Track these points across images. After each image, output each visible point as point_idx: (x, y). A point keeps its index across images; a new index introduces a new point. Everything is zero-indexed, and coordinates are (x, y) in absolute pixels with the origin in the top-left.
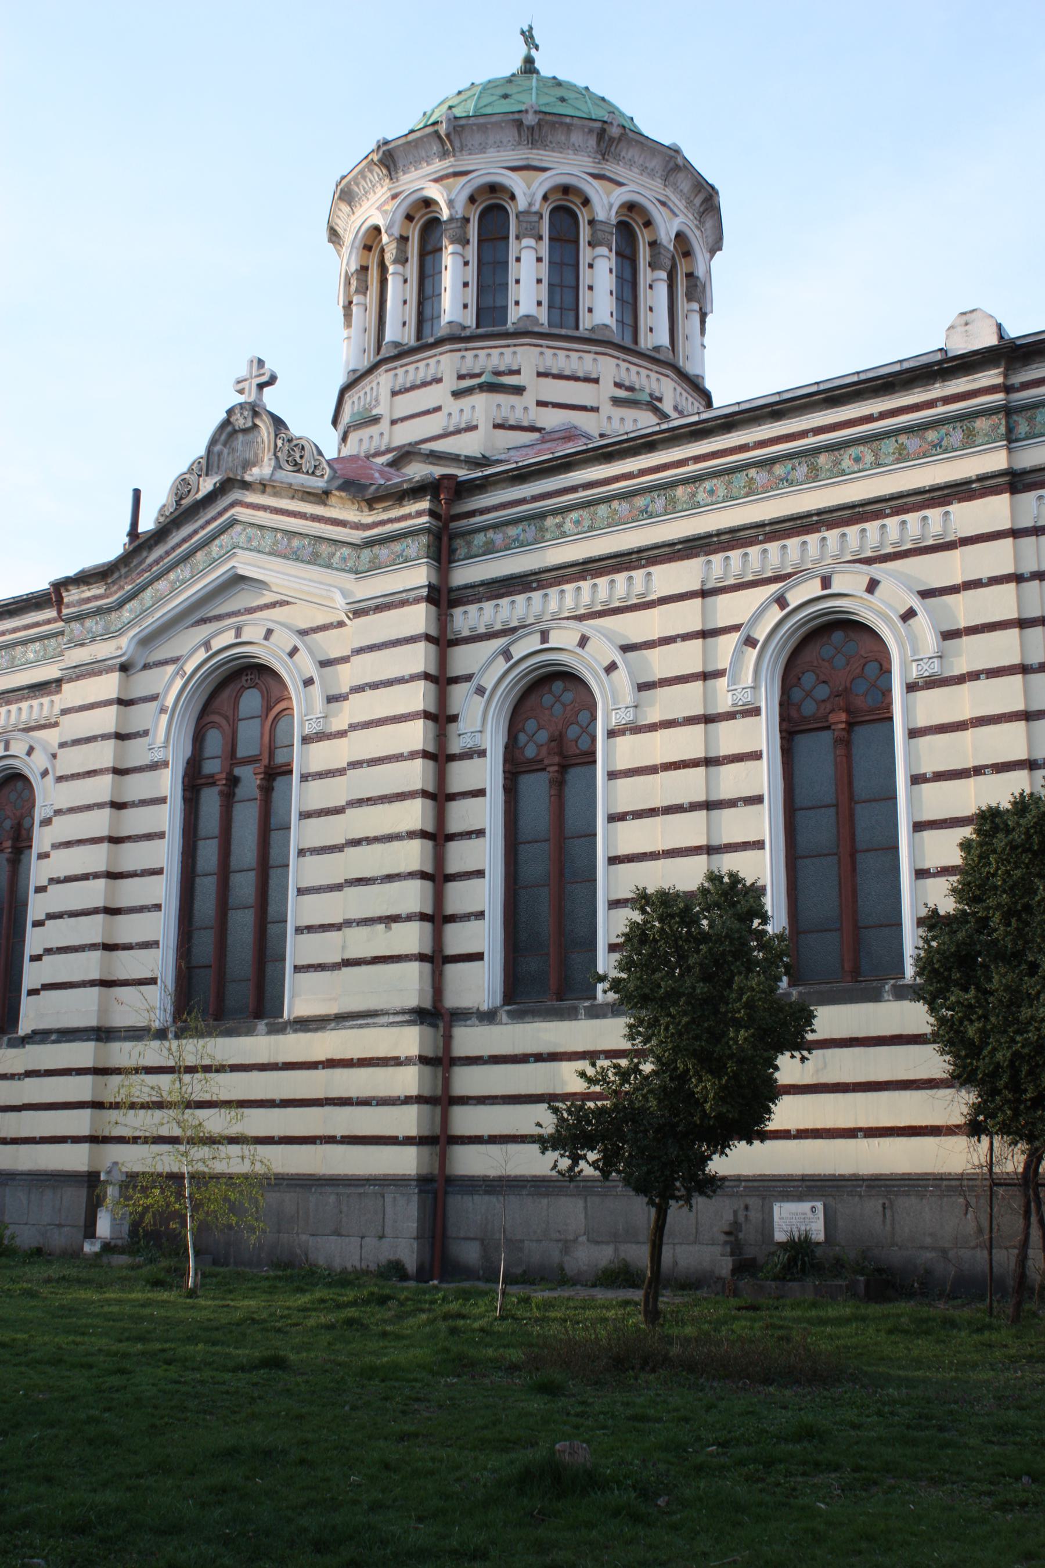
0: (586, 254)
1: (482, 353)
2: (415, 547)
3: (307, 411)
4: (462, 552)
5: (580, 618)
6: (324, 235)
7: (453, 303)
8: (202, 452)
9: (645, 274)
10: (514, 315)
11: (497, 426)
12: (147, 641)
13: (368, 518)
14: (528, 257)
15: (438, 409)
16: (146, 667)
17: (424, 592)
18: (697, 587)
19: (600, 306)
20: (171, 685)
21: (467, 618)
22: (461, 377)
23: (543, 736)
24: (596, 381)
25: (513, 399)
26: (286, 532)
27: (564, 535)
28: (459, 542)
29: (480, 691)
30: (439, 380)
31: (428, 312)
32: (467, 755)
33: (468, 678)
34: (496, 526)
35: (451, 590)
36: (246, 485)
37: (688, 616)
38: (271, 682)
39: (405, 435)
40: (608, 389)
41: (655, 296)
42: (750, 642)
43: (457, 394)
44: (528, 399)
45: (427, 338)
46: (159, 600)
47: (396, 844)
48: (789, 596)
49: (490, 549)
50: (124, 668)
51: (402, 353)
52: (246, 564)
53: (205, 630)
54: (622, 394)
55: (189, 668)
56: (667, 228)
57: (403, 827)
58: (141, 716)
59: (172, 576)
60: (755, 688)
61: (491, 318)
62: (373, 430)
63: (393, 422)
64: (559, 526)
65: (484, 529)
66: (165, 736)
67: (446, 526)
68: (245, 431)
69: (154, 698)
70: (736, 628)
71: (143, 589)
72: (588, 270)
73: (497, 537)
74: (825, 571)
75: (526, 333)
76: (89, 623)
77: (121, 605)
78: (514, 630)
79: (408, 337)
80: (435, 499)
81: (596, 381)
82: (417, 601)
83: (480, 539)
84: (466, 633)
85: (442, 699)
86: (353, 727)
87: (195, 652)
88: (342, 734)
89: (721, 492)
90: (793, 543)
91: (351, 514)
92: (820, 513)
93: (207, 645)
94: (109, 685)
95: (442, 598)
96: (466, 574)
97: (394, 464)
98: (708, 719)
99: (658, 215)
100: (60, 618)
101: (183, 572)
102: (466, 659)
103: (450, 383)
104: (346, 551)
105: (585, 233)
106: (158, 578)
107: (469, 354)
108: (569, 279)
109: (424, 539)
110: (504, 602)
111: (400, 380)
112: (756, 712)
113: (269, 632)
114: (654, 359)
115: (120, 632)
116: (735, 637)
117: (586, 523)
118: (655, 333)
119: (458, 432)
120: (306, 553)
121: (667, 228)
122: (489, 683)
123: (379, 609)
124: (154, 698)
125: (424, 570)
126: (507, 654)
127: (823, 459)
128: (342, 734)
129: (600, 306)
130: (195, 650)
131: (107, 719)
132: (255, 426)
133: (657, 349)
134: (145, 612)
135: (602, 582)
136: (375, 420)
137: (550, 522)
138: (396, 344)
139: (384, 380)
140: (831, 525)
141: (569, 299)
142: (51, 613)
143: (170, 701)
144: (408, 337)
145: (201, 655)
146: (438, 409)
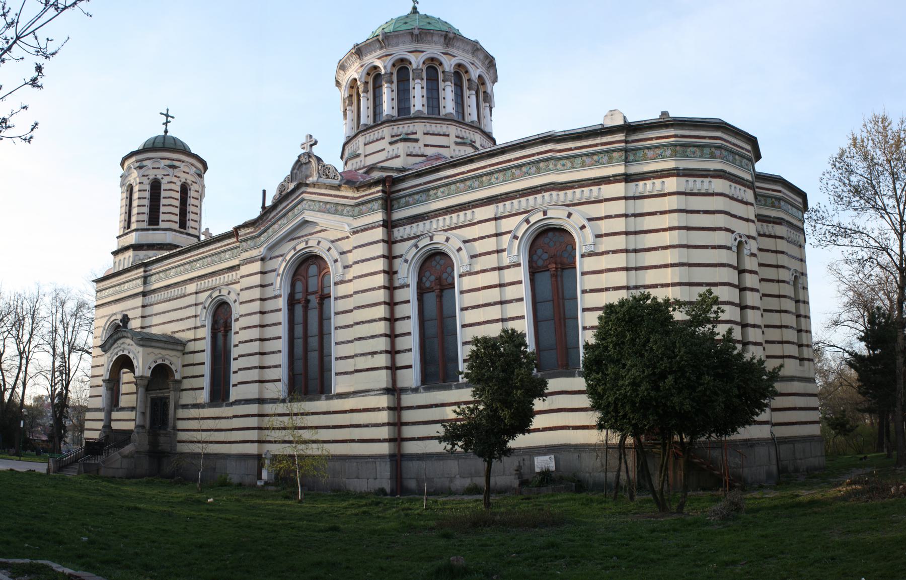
0: (441, 85)
1: (401, 126)
2: (376, 205)
3: (330, 154)
4: (396, 206)
5: (446, 230)
6: (334, 83)
7: (388, 106)
8: (289, 173)
9: (466, 92)
10: (413, 111)
11: (408, 155)
12: (271, 248)
13: (357, 195)
14: (418, 87)
15: (384, 150)
16: (271, 258)
17: (381, 223)
18: (493, 216)
19: (448, 105)
20: (281, 265)
21: (399, 233)
22: (392, 136)
23: (433, 278)
24: (448, 135)
25: (414, 144)
26: (324, 202)
27: (438, 197)
28: (395, 202)
29: (406, 261)
30: (383, 138)
31: (378, 111)
32: (402, 287)
33: (401, 256)
34: (409, 195)
35: (392, 221)
36: (307, 185)
37: (490, 228)
38: (321, 262)
39: (370, 161)
40: (452, 139)
41: (471, 101)
42: (516, 237)
43: (391, 143)
44: (421, 144)
45: (378, 121)
46: (275, 232)
47: (374, 323)
48: (530, 219)
49: (407, 204)
50: (262, 259)
51: (368, 128)
52: (308, 216)
53: (293, 243)
54: (459, 140)
55: (288, 258)
56: (474, 73)
57: (377, 316)
58: (270, 278)
59: (279, 223)
60: (518, 255)
61: (404, 112)
62: (358, 160)
63: (366, 156)
64: (436, 194)
65: (405, 196)
66: (280, 285)
67: (389, 196)
68: (306, 164)
69: (274, 270)
70: (510, 232)
71: (268, 228)
73: (410, 200)
74: (545, 209)
75: (418, 117)
76: (249, 242)
77: (260, 235)
78: (419, 236)
79: (370, 122)
80: (384, 185)
81: (448, 135)
82: (378, 226)
83: (403, 201)
84: (399, 238)
85: (391, 265)
86: (355, 278)
87: (289, 252)
88: (350, 281)
89: (501, 179)
90: (531, 198)
91: (350, 193)
92: (541, 186)
93: (294, 248)
94: (257, 266)
95: (389, 225)
96: (397, 215)
97: (367, 173)
98: (500, 269)
99: (471, 68)
100: (238, 241)
101: (284, 221)
102: (399, 249)
103: (388, 139)
104: (348, 208)
105: (441, 76)
106: (274, 224)
107: (395, 127)
108: (435, 95)
109: (380, 202)
110: (414, 225)
111: (368, 139)
112: (519, 265)
113: (319, 242)
114: (472, 126)
115: (260, 246)
116: (509, 236)
117: (447, 193)
118: (471, 115)
119: (392, 158)
120: (332, 210)
121: (474, 73)
122: (409, 257)
123: (363, 230)
124: (274, 270)
125: (381, 214)
126: (416, 246)
127: (541, 165)
128: (350, 281)
130: (290, 251)
131: (257, 280)
132: (310, 161)
133: (472, 122)
134: (269, 237)
135: (454, 216)
136: (358, 156)
137: (432, 192)
138: (365, 125)
139: (361, 140)
140: (546, 191)
141: (435, 103)
142: (234, 240)
143: (281, 271)
144: (370, 122)
145: (293, 253)
146: (384, 150)
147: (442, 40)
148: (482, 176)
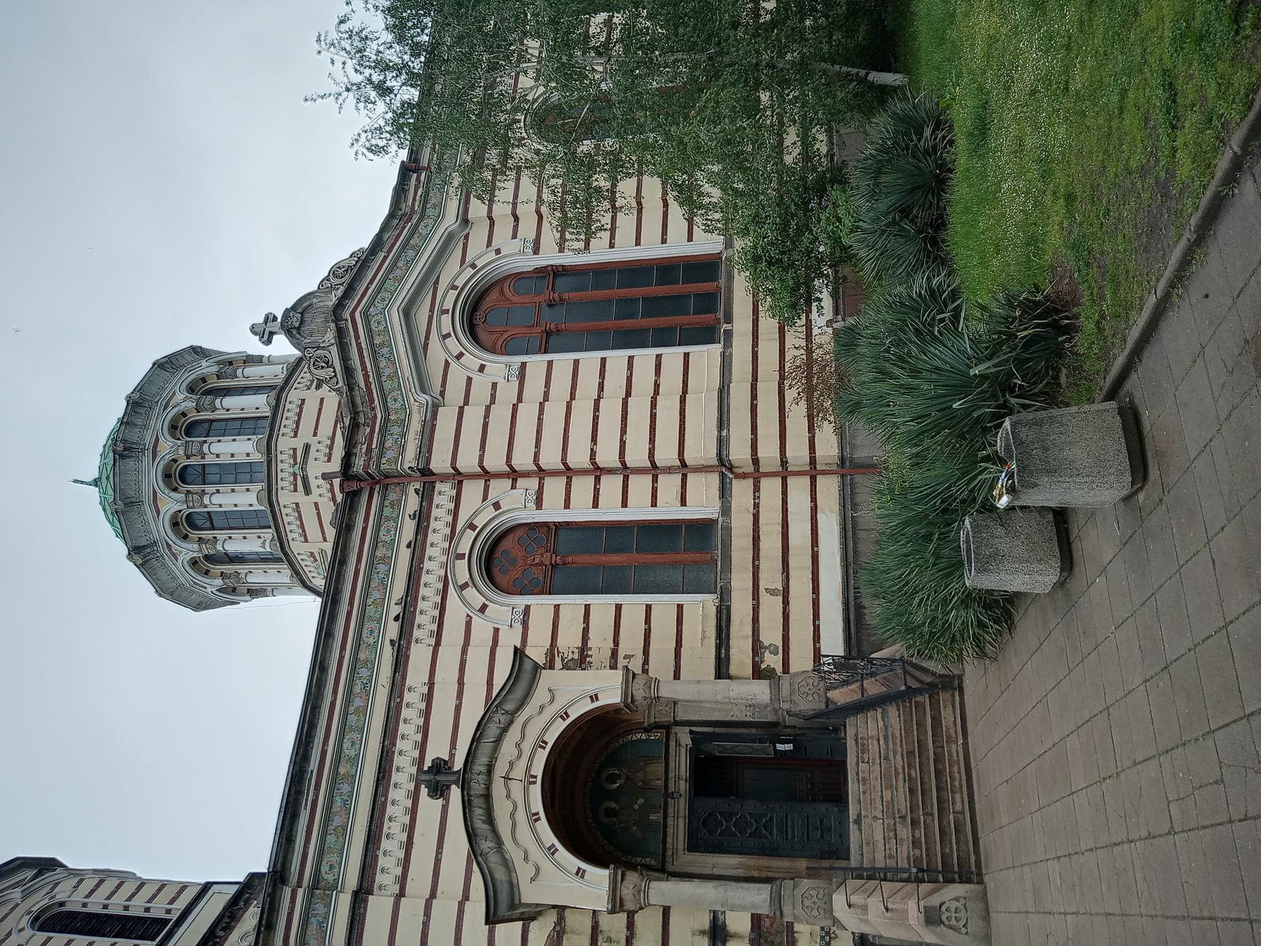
0: (210, 459)
14: (217, 499)
15: (316, 504)
19: (242, 448)
22: (295, 490)
41: (234, 405)
43: (307, 491)
72: (222, 458)
103: (300, 497)
118: (258, 404)
129: (242, 448)
139: (297, 548)
147: (131, 463)
148: (372, 345)
